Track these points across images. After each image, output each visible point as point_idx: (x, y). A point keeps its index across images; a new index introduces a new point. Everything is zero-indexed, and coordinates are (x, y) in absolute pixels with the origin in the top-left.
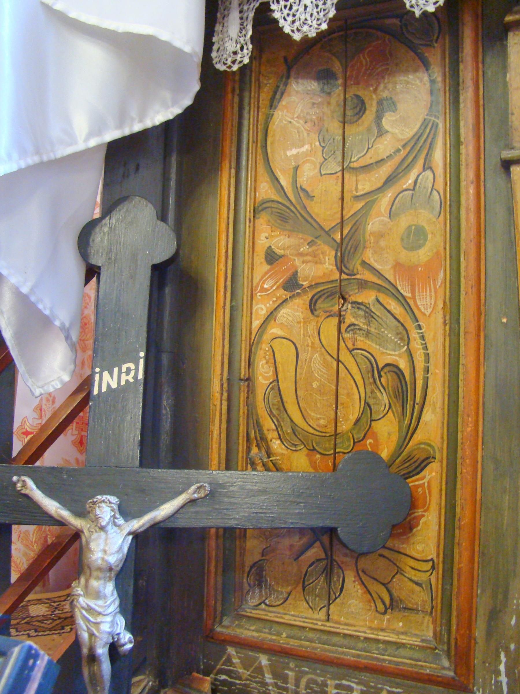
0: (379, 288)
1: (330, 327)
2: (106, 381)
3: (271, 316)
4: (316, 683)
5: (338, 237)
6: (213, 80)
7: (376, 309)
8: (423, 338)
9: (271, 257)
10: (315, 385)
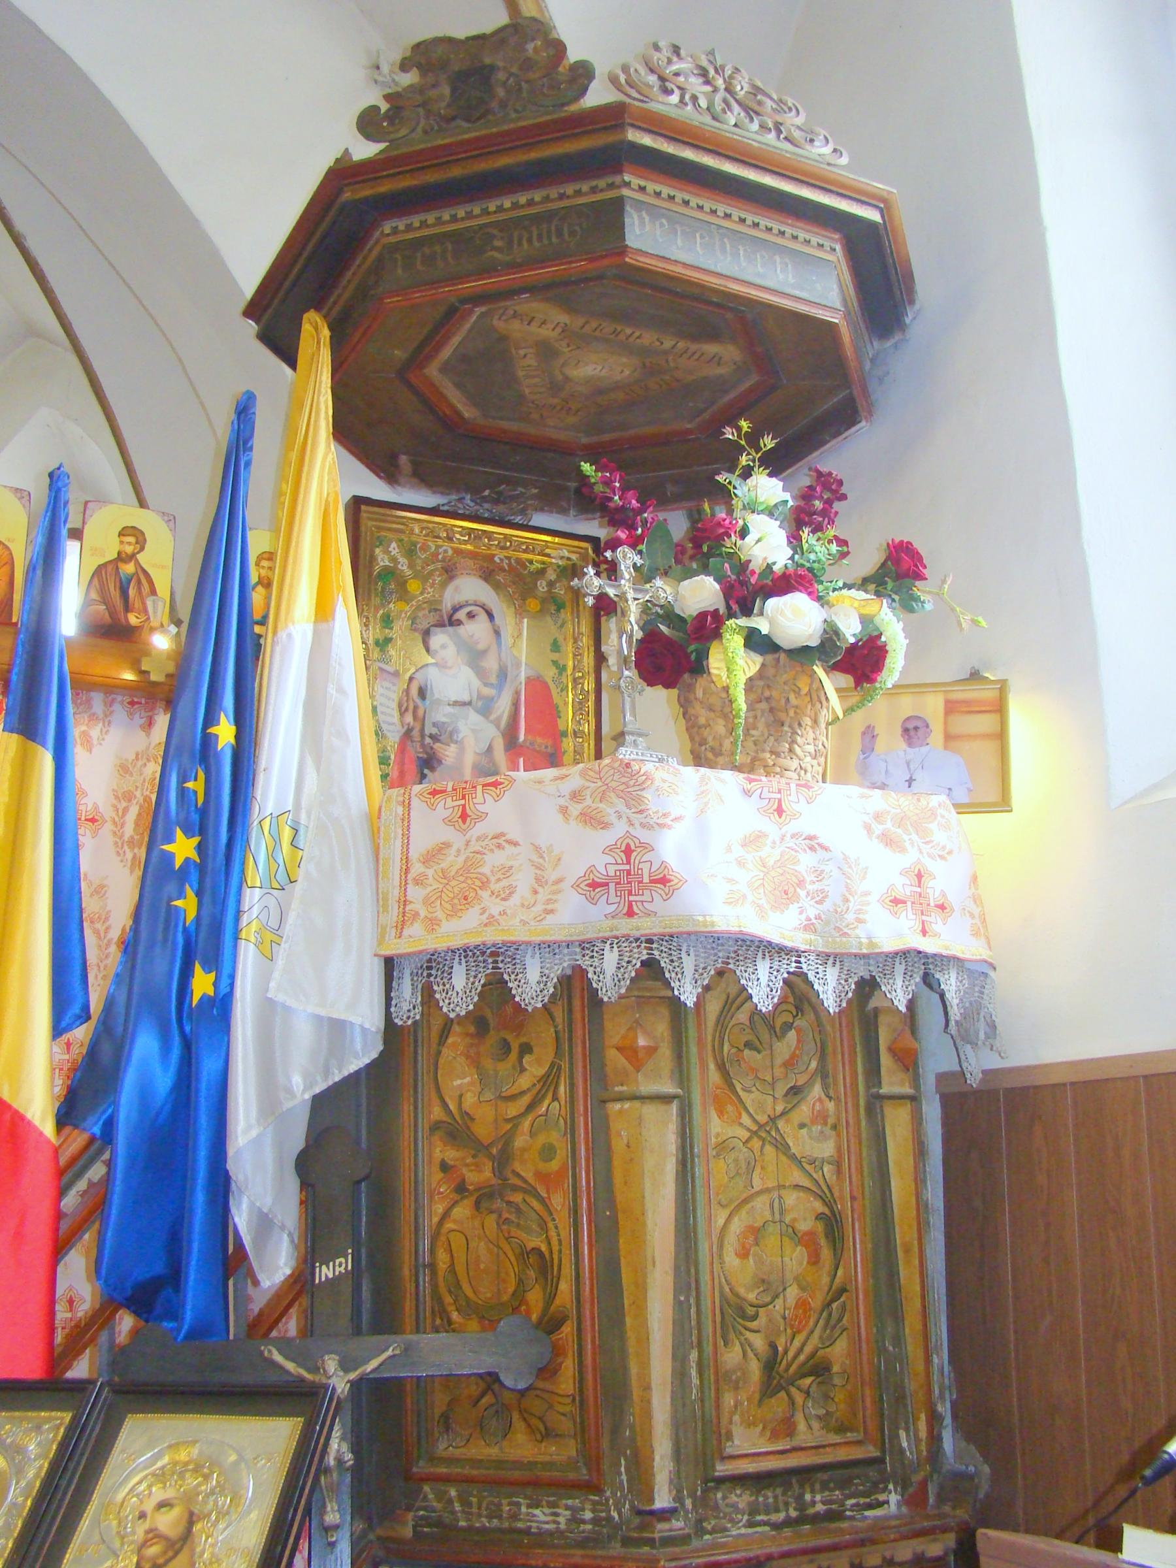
0: (525, 1191)
1: (491, 1221)
2: (325, 1272)
3: (446, 1215)
4: (492, 1503)
5: (494, 1151)
6: (391, 1031)
7: (523, 1206)
8: (556, 1227)
9: (444, 1167)
10: (482, 1266)
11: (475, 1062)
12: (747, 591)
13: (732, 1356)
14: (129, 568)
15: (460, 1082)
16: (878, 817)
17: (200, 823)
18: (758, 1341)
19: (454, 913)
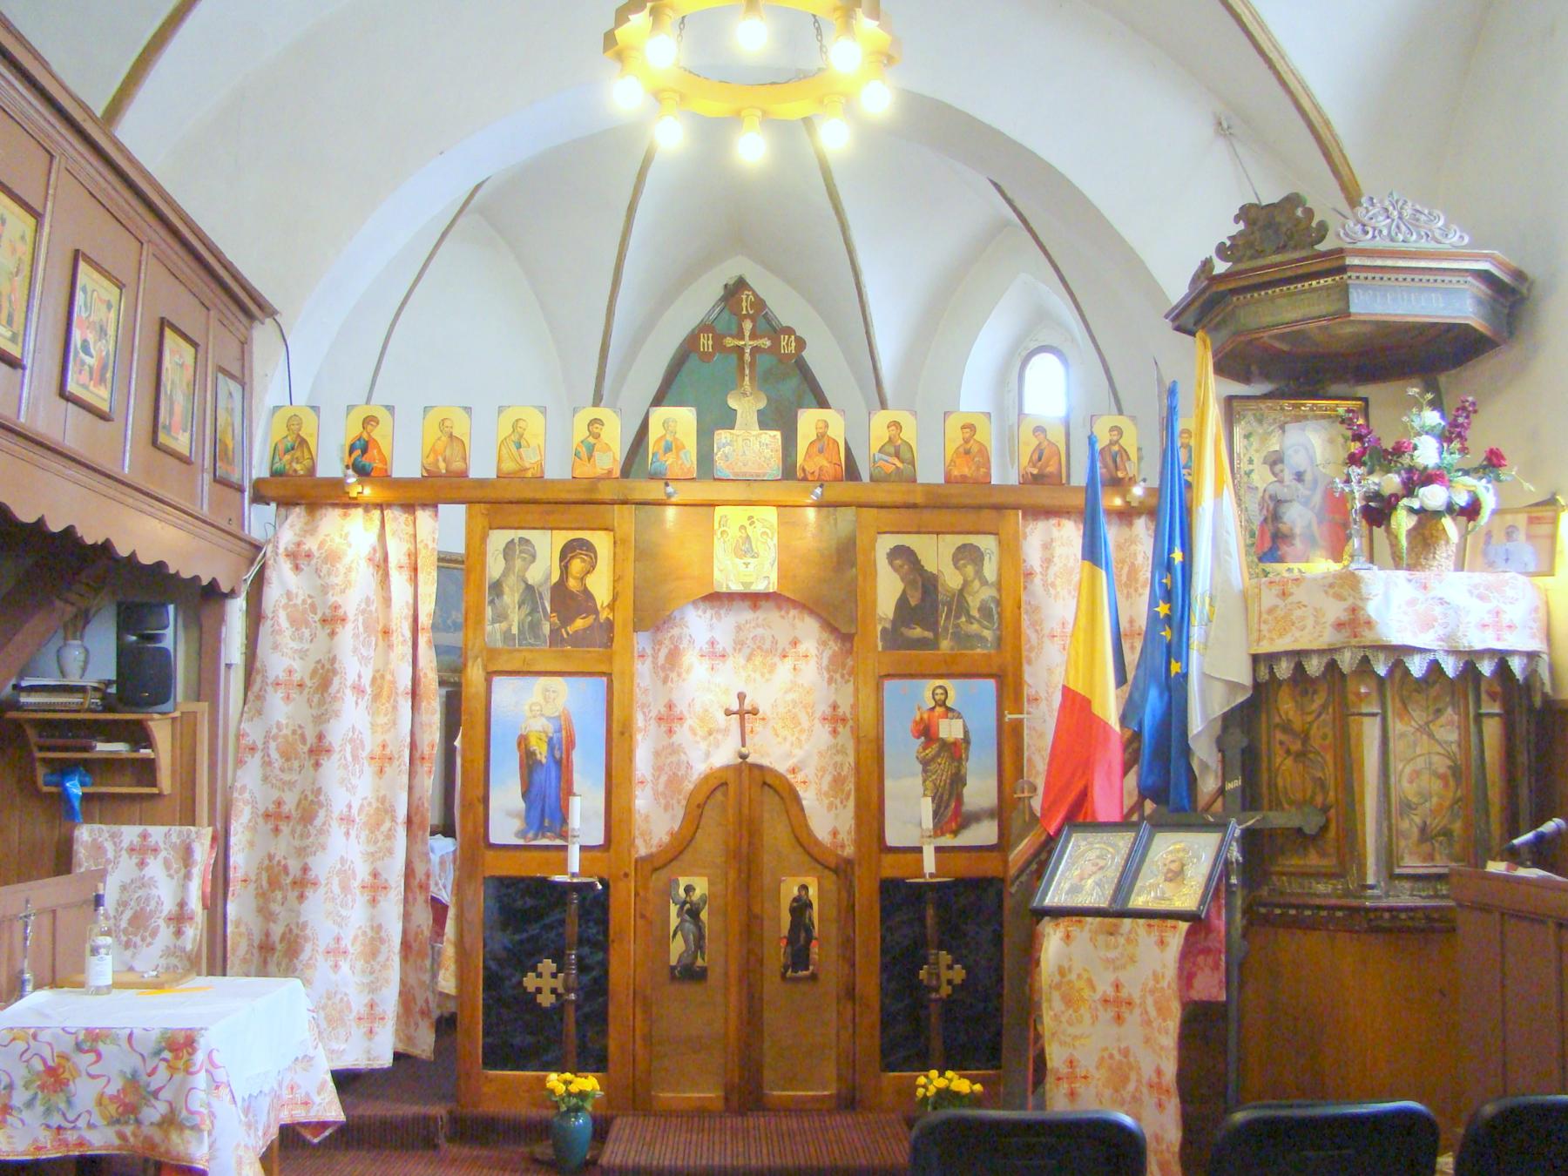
2: (1230, 786)
6: (1257, 685)
11: (1294, 698)
12: (1418, 479)
13: (1405, 825)
14: (1116, 448)
15: (1286, 706)
16: (1476, 586)
17: (1168, 596)
18: (1417, 820)
19: (1281, 635)
